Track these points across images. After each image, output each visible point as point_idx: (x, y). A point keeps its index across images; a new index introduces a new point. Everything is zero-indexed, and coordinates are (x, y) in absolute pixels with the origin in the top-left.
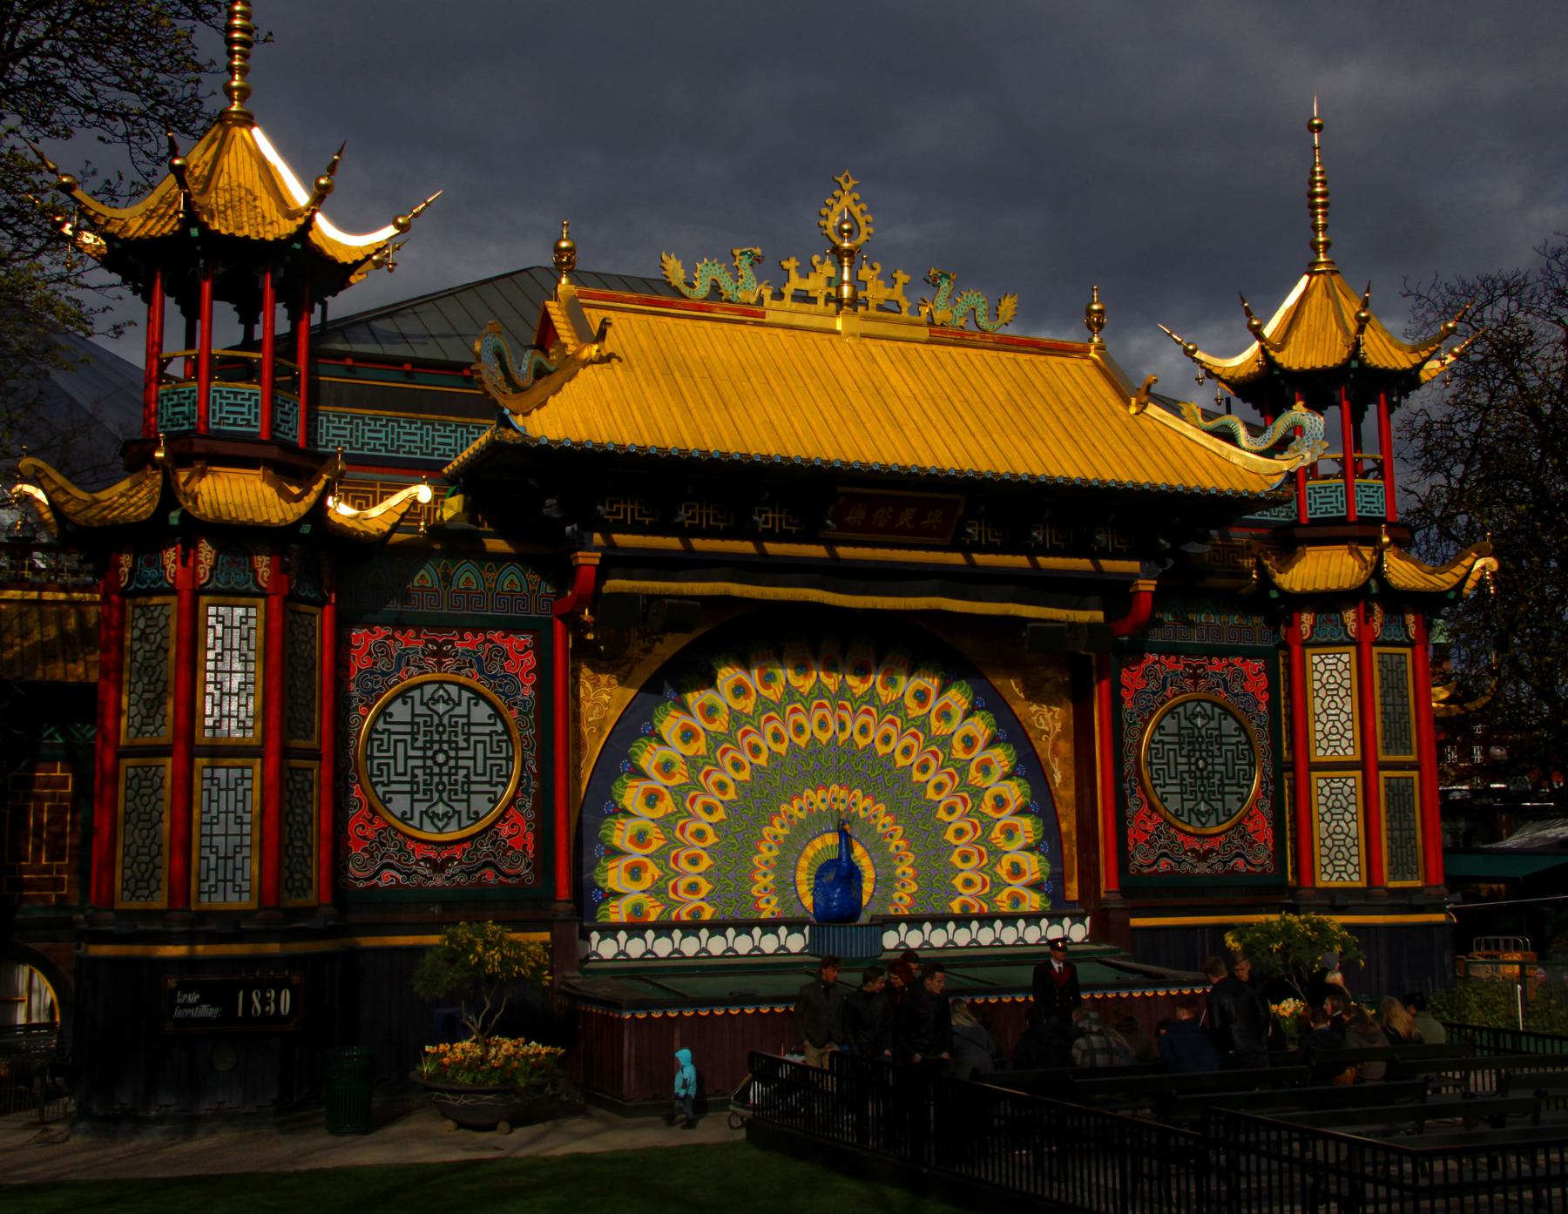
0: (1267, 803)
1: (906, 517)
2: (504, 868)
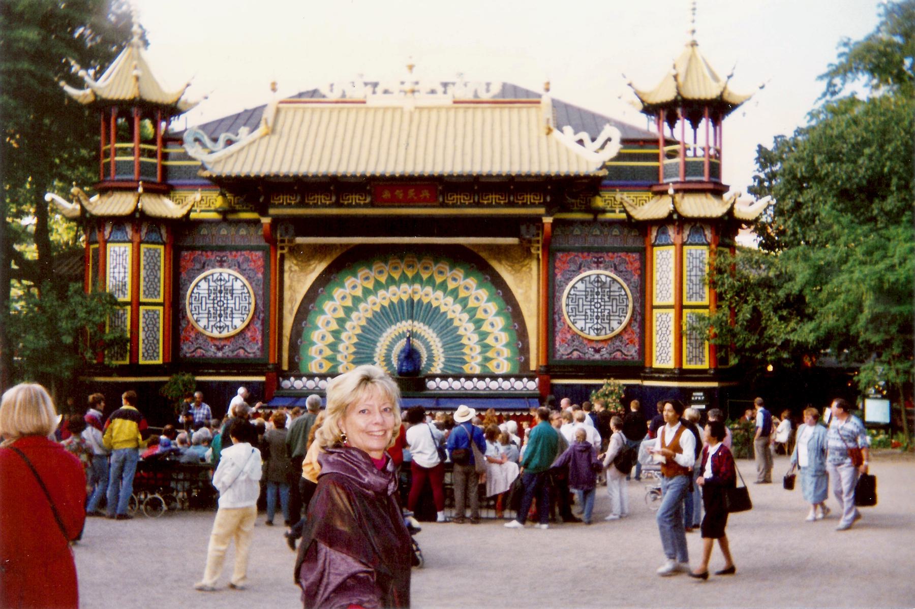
0: (637, 325)
1: (411, 193)
2: (249, 350)
